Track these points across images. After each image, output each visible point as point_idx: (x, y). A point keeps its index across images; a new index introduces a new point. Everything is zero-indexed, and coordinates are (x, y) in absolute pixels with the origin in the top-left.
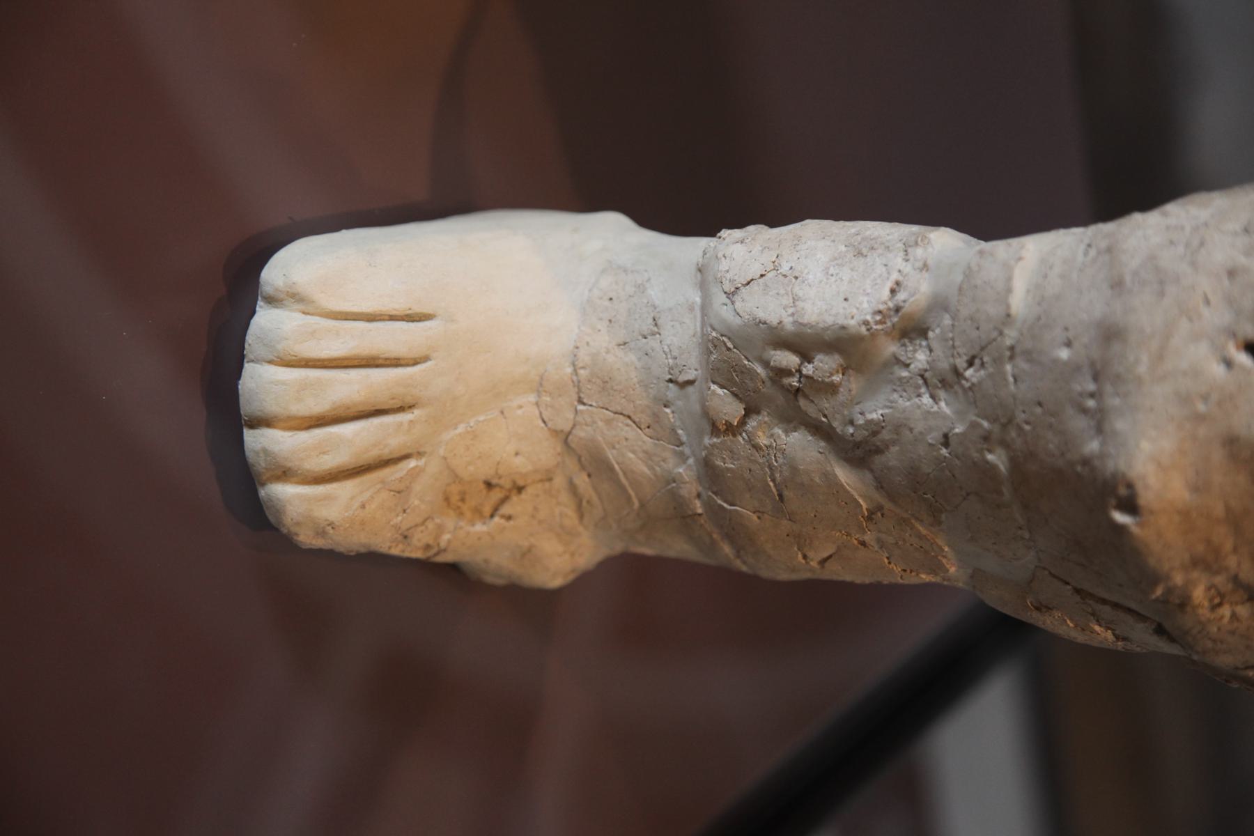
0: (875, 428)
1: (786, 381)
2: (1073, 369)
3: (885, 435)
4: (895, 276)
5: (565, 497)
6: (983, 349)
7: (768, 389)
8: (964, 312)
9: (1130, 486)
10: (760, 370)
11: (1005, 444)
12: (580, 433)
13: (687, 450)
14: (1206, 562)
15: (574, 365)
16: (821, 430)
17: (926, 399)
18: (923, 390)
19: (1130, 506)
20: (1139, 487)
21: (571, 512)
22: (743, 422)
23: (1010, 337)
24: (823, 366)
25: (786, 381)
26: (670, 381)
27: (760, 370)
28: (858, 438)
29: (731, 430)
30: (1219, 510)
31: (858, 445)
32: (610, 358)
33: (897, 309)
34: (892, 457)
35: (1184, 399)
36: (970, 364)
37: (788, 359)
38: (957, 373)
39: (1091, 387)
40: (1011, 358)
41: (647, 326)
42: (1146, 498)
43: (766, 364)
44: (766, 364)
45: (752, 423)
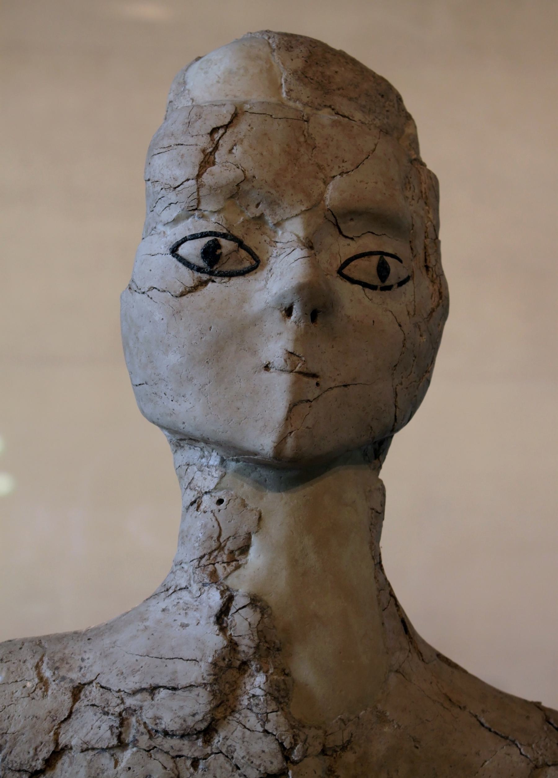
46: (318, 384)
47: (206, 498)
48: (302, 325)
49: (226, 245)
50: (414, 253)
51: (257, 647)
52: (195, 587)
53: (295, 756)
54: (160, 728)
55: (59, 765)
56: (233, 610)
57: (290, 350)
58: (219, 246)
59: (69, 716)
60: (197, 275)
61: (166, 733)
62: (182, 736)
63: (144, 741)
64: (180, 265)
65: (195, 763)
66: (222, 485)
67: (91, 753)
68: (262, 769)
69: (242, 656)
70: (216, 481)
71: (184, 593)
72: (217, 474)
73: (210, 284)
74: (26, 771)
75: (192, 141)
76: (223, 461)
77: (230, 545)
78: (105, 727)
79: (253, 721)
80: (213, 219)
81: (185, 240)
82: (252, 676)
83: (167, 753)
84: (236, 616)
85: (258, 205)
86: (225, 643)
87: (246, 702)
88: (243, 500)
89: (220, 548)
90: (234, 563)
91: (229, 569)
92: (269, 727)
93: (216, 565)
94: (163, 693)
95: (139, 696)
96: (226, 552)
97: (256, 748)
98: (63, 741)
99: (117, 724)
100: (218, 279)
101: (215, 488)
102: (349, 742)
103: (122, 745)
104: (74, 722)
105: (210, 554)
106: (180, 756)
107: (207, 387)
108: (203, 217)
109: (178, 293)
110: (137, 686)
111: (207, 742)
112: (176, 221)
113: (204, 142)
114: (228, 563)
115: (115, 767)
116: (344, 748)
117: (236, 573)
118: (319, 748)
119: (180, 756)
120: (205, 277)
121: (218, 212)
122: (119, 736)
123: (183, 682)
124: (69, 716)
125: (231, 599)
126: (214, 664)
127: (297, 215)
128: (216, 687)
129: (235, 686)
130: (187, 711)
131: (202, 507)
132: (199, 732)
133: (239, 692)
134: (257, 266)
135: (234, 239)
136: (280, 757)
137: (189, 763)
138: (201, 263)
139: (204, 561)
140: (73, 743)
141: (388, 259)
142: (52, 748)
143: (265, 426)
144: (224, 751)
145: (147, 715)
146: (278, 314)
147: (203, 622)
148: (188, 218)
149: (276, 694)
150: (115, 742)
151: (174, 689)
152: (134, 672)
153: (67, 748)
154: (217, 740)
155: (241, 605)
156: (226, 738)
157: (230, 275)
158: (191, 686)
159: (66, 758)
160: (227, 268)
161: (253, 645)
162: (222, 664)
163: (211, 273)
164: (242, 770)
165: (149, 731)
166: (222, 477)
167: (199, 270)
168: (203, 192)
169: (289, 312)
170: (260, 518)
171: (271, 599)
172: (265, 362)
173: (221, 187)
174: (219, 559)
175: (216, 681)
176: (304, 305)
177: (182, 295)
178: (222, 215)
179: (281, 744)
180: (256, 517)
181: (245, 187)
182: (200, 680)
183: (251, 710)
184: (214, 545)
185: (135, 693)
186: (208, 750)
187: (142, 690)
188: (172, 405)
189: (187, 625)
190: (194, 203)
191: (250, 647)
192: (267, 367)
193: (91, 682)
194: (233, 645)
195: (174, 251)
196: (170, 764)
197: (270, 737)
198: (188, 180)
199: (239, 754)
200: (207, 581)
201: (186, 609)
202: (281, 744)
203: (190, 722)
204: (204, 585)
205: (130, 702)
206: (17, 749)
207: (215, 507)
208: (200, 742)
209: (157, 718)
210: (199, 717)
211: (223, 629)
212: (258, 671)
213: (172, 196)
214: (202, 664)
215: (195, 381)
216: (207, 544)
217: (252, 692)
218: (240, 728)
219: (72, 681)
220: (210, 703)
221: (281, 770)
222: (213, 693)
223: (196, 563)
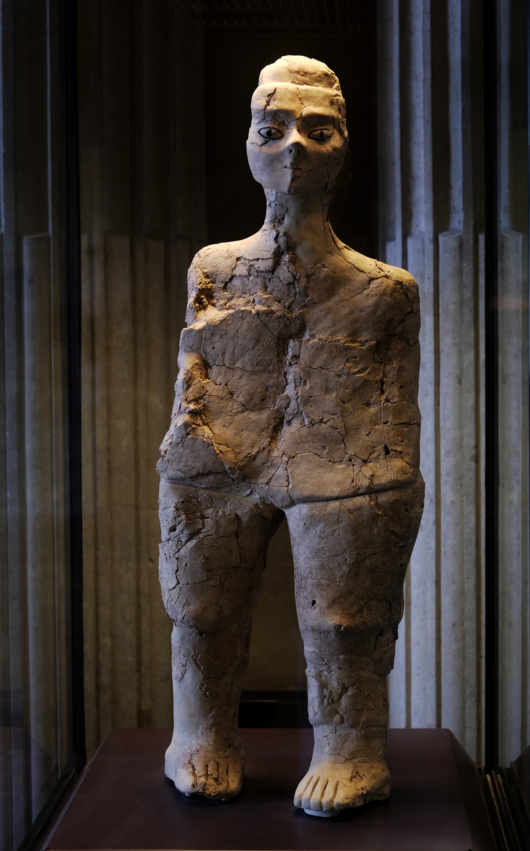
0: (339, 684)
1: (330, 702)
2: (320, 638)
3: (340, 682)
4: (312, 678)
5: (362, 764)
6: (320, 658)
7: (333, 706)
8: (315, 662)
9: (336, 626)
10: (328, 708)
11: (338, 655)
12: (346, 756)
13: (350, 732)
14: (353, 616)
15: (331, 755)
16: (340, 696)
17: (333, 672)
18: (331, 673)
19: (340, 626)
20: (337, 624)
21: (366, 765)
22: (341, 715)
23: (317, 651)
24: (326, 692)
25: (330, 702)
26: (335, 733)
27: (328, 708)
28: (341, 688)
29: (342, 718)
30: (341, 612)
31: (343, 689)
32: (331, 747)
33: (316, 676)
34: (345, 681)
35: (321, 616)
36: (324, 661)
37: (326, 700)
38: (326, 664)
39: (323, 634)
40: (322, 652)
41: (326, 738)
42: (338, 623)
43: (327, 706)
44: (327, 706)
45: (340, 712)
46: (301, 171)
47: (272, 203)
48: (295, 155)
49: (273, 131)
50: (335, 125)
51: (286, 247)
52: (269, 230)
53: (297, 278)
54: (260, 270)
55: (233, 280)
56: (279, 237)
57: (292, 162)
58: (271, 131)
59: (235, 267)
60: (265, 139)
61: (262, 272)
62: (266, 273)
63: (256, 274)
64: (261, 136)
65: (270, 280)
66: (276, 200)
67: (241, 277)
68: (288, 281)
69: (282, 250)
70: (275, 199)
71: (267, 231)
72: (275, 196)
73: (269, 142)
74: (224, 282)
75: (263, 98)
76: (276, 193)
77: (279, 218)
78: (245, 269)
79: (285, 268)
80: (269, 122)
81: (261, 129)
82: (285, 255)
83: (262, 277)
84: (280, 238)
85: (282, 118)
86: (277, 246)
87: (283, 263)
88: (282, 204)
89: (276, 218)
90: (280, 223)
91: (279, 225)
92: (289, 270)
93: (275, 223)
94: (260, 260)
95: (254, 261)
96: (278, 219)
97: (286, 276)
98: (234, 273)
99: (248, 269)
100: (272, 140)
101: (274, 201)
102: (314, 273)
103: (250, 275)
104: (237, 269)
105: (273, 220)
106: (266, 278)
107: (269, 173)
108: (266, 121)
109: (260, 144)
110: (253, 258)
111: (273, 274)
112: (259, 123)
113: (267, 98)
114: (279, 223)
115: (248, 281)
116: (312, 275)
117: (281, 226)
118: (305, 275)
119: (266, 278)
120: (268, 140)
121: (271, 120)
122: (249, 272)
123: (266, 258)
124: (235, 267)
125: (279, 233)
126: (274, 252)
127: (294, 121)
128: (275, 259)
129: (280, 258)
130: (267, 265)
131: (271, 206)
132: (270, 272)
133: (281, 260)
134: (283, 136)
135: (275, 129)
136: (293, 278)
137: (268, 280)
138: (266, 136)
139: (272, 222)
140: (237, 274)
141: (324, 131)
142: (231, 276)
143: (285, 184)
144: (277, 276)
145: (256, 266)
146: (288, 152)
147: (271, 240)
148: (262, 122)
149: (292, 260)
150: (248, 274)
151: (263, 259)
152: (253, 255)
153: (235, 275)
154: (276, 273)
155: (281, 235)
156: (278, 273)
157: (275, 139)
158: (268, 258)
159: (234, 278)
160: (274, 137)
161: (285, 247)
162: (276, 252)
163: (269, 139)
164: (282, 282)
165: (257, 271)
166: (276, 197)
167: (266, 138)
168: (266, 114)
169: (291, 151)
170: (287, 210)
171: (290, 234)
172: (285, 166)
173: (271, 113)
174: (276, 222)
175: (274, 257)
176: (295, 150)
177: (261, 145)
178: (272, 121)
179: (293, 275)
180: (286, 209)
181: (278, 113)
182: (270, 257)
183: (285, 265)
184: (274, 218)
185: (253, 260)
186: (273, 276)
187: (255, 260)
188: (260, 177)
189: (267, 241)
190: (264, 118)
191: (284, 247)
192: (286, 167)
193: (241, 257)
194: (279, 247)
195: (259, 132)
196: (263, 280)
197: (290, 273)
198: (261, 111)
199: (281, 277)
200: (272, 228)
201: (267, 235)
202: (293, 275)
203: (268, 268)
204: (272, 229)
205: (252, 263)
206: (221, 276)
207: (274, 206)
208: (271, 274)
209: (259, 267)
210: (270, 267)
211: (277, 242)
212: (287, 254)
213: (258, 115)
214: (271, 252)
215: (266, 171)
216: (273, 217)
217: (285, 260)
218: (282, 270)
219: (236, 257)
220: (273, 263)
221: (293, 282)
222: (274, 260)
223: (269, 223)
